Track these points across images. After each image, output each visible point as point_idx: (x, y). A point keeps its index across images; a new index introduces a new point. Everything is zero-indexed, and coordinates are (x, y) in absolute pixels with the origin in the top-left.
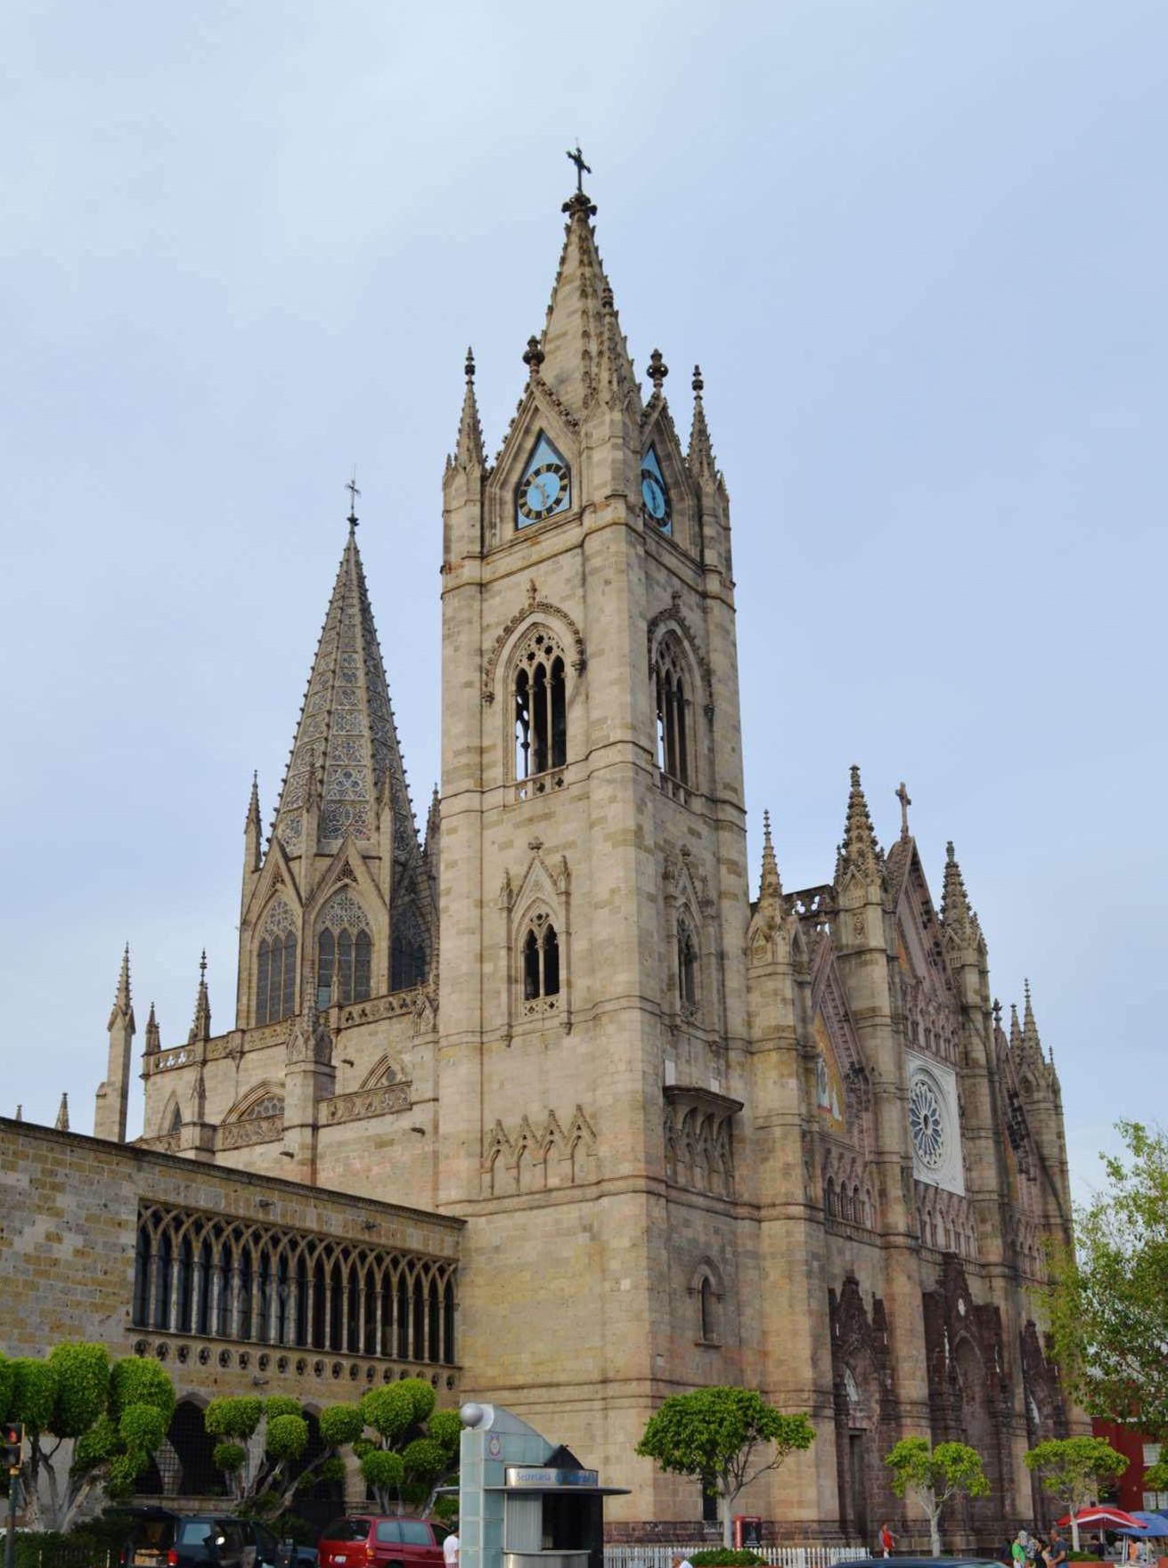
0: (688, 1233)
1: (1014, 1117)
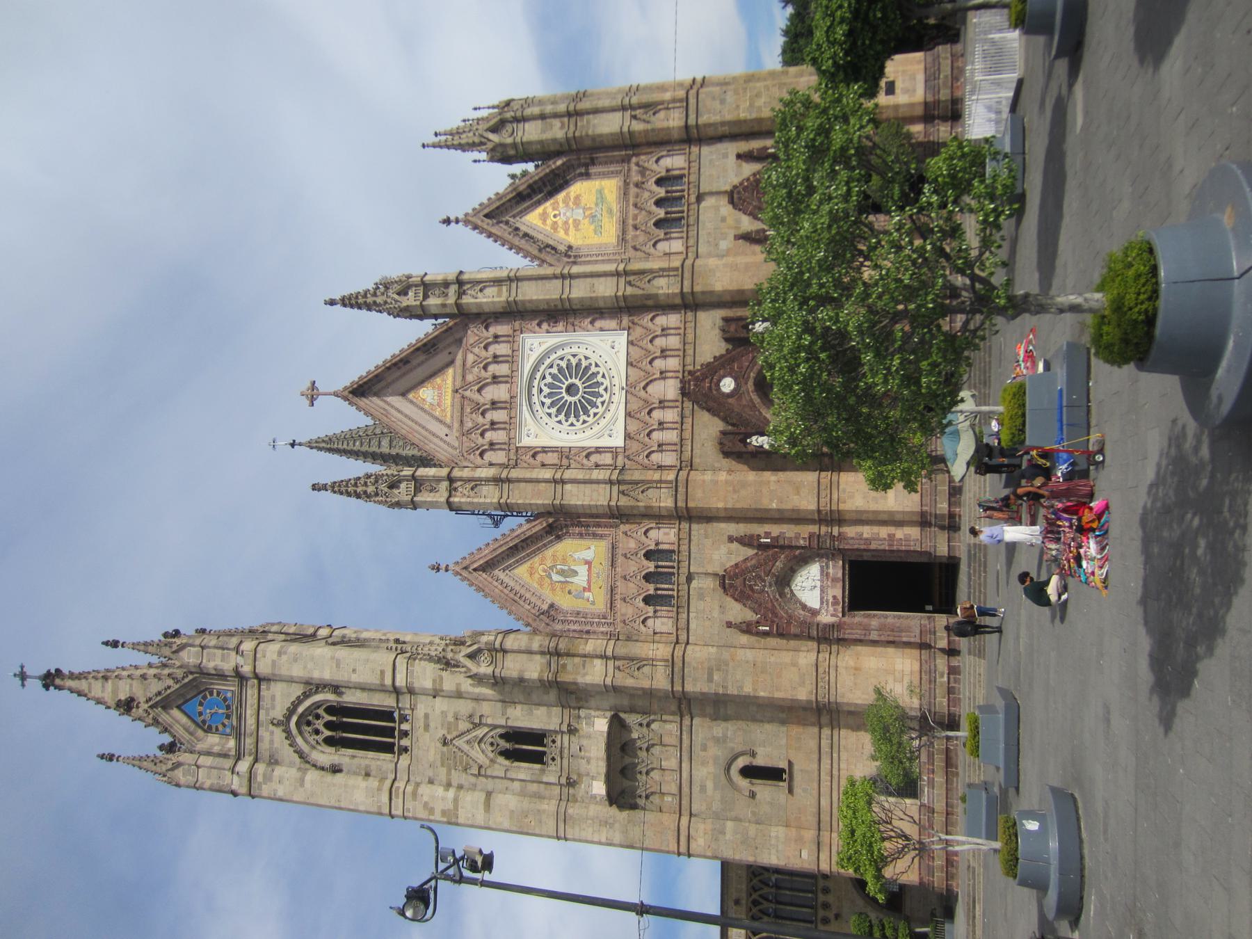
0: (710, 785)
1: (541, 192)
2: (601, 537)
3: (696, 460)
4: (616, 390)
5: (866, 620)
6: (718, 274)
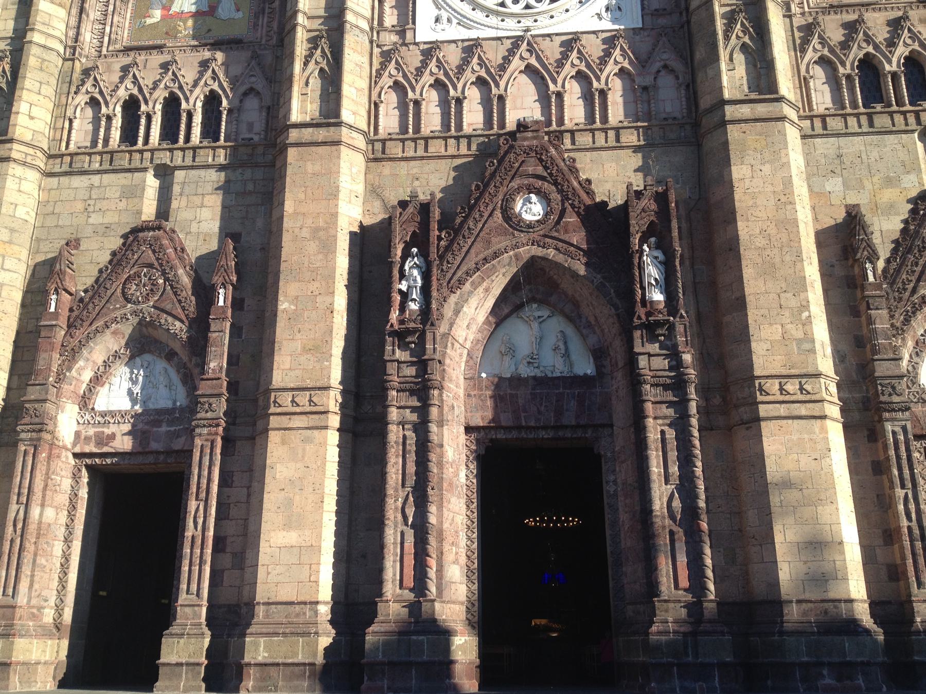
2: (255, 25)
3: (387, 168)
4: (527, 22)
5: (63, 499)
6: (767, 169)
